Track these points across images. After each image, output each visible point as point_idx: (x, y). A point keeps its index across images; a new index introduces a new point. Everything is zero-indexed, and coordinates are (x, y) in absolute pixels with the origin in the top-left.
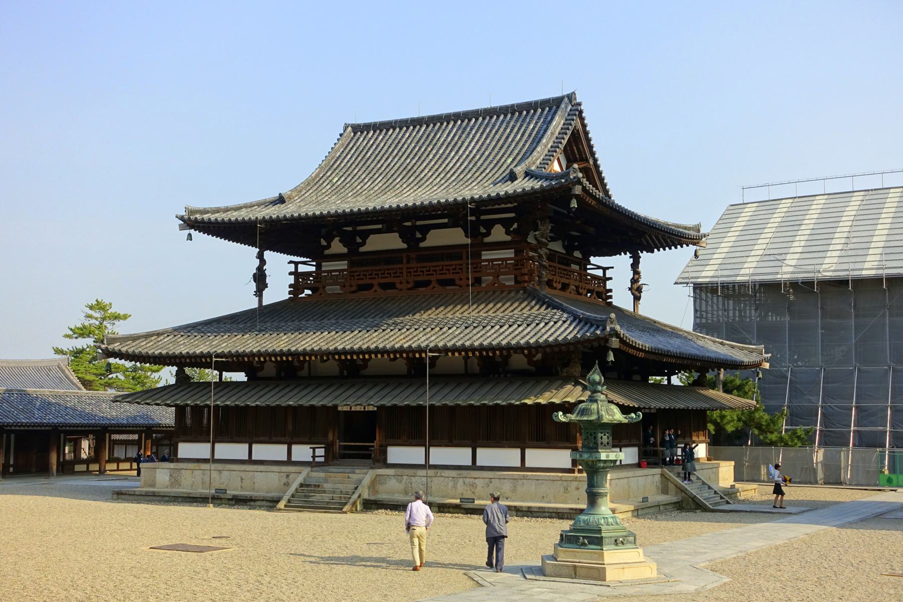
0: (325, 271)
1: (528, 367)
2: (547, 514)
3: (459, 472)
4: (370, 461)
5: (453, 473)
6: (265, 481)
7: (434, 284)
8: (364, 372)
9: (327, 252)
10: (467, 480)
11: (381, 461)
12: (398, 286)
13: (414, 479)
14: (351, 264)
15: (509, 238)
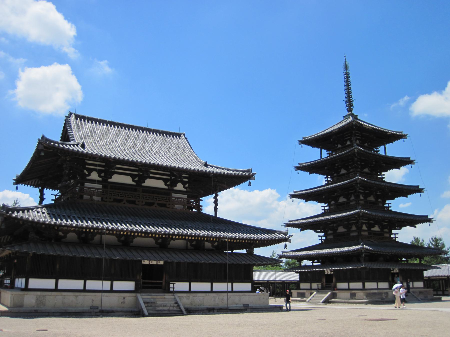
0: (86, 187)
1: (212, 248)
2: (47, 314)
3: (217, 294)
4: (161, 290)
5: (204, 294)
6: (110, 301)
7: (156, 205)
8: (131, 244)
9: (88, 178)
10: (220, 297)
11: (167, 290)
12: (137, 203)
13: (195, 298)
14: (104, 187)
15: (185, 190)
